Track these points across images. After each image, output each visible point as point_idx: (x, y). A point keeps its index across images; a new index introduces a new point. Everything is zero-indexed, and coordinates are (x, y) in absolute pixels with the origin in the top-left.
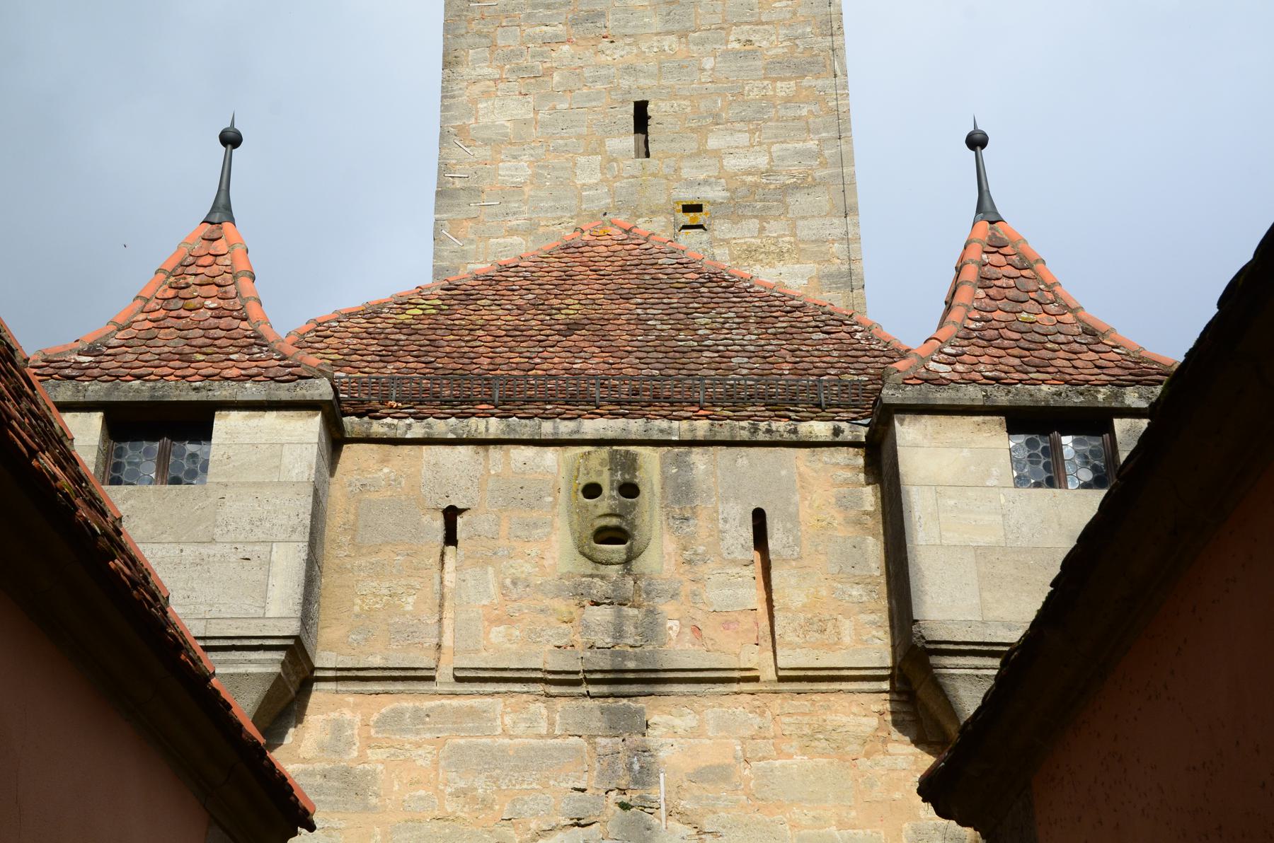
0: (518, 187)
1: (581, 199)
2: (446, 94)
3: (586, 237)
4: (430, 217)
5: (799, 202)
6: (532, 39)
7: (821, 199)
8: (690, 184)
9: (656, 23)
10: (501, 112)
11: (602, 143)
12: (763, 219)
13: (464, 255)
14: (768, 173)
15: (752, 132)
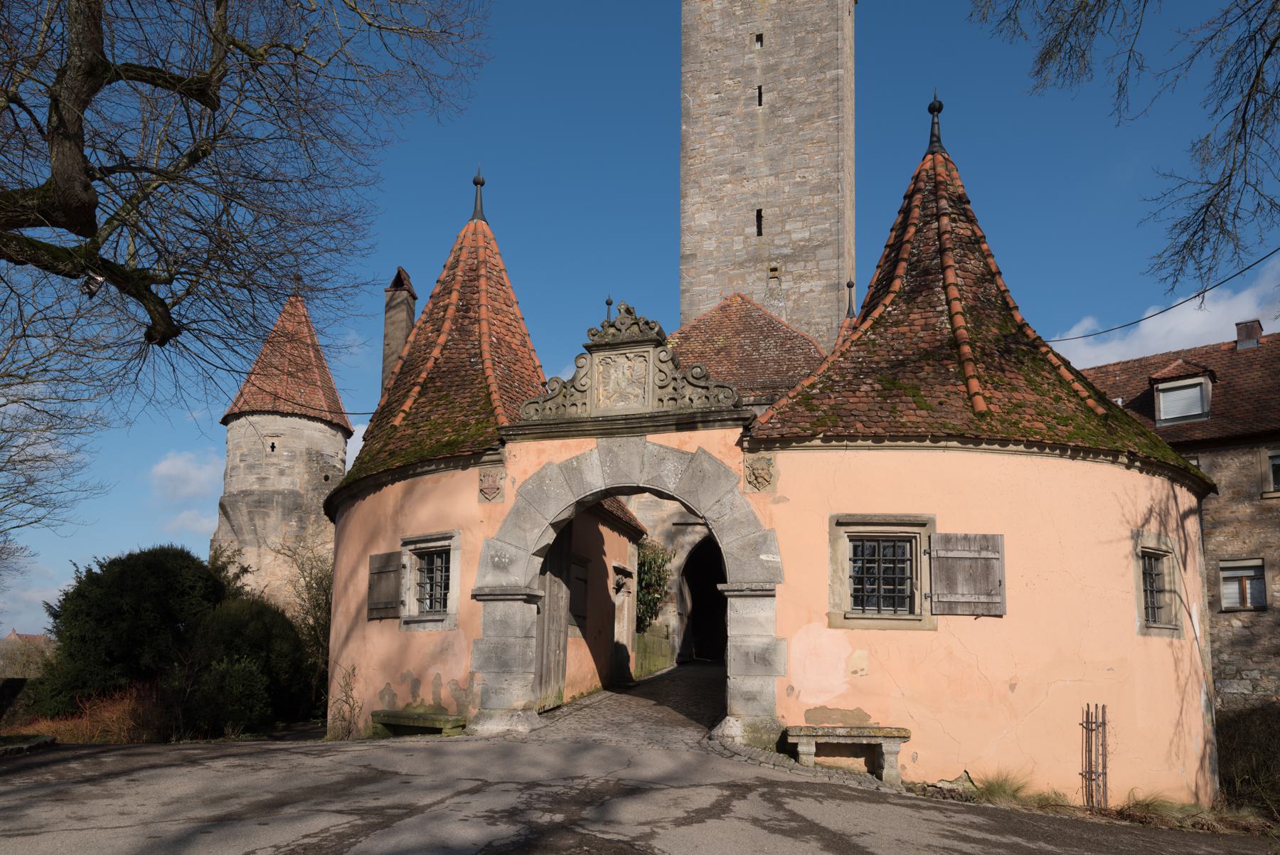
5: (821, 253)
7: (829, 251)
8: (778, 247)
13: (691, 284)
14: (809, 240)
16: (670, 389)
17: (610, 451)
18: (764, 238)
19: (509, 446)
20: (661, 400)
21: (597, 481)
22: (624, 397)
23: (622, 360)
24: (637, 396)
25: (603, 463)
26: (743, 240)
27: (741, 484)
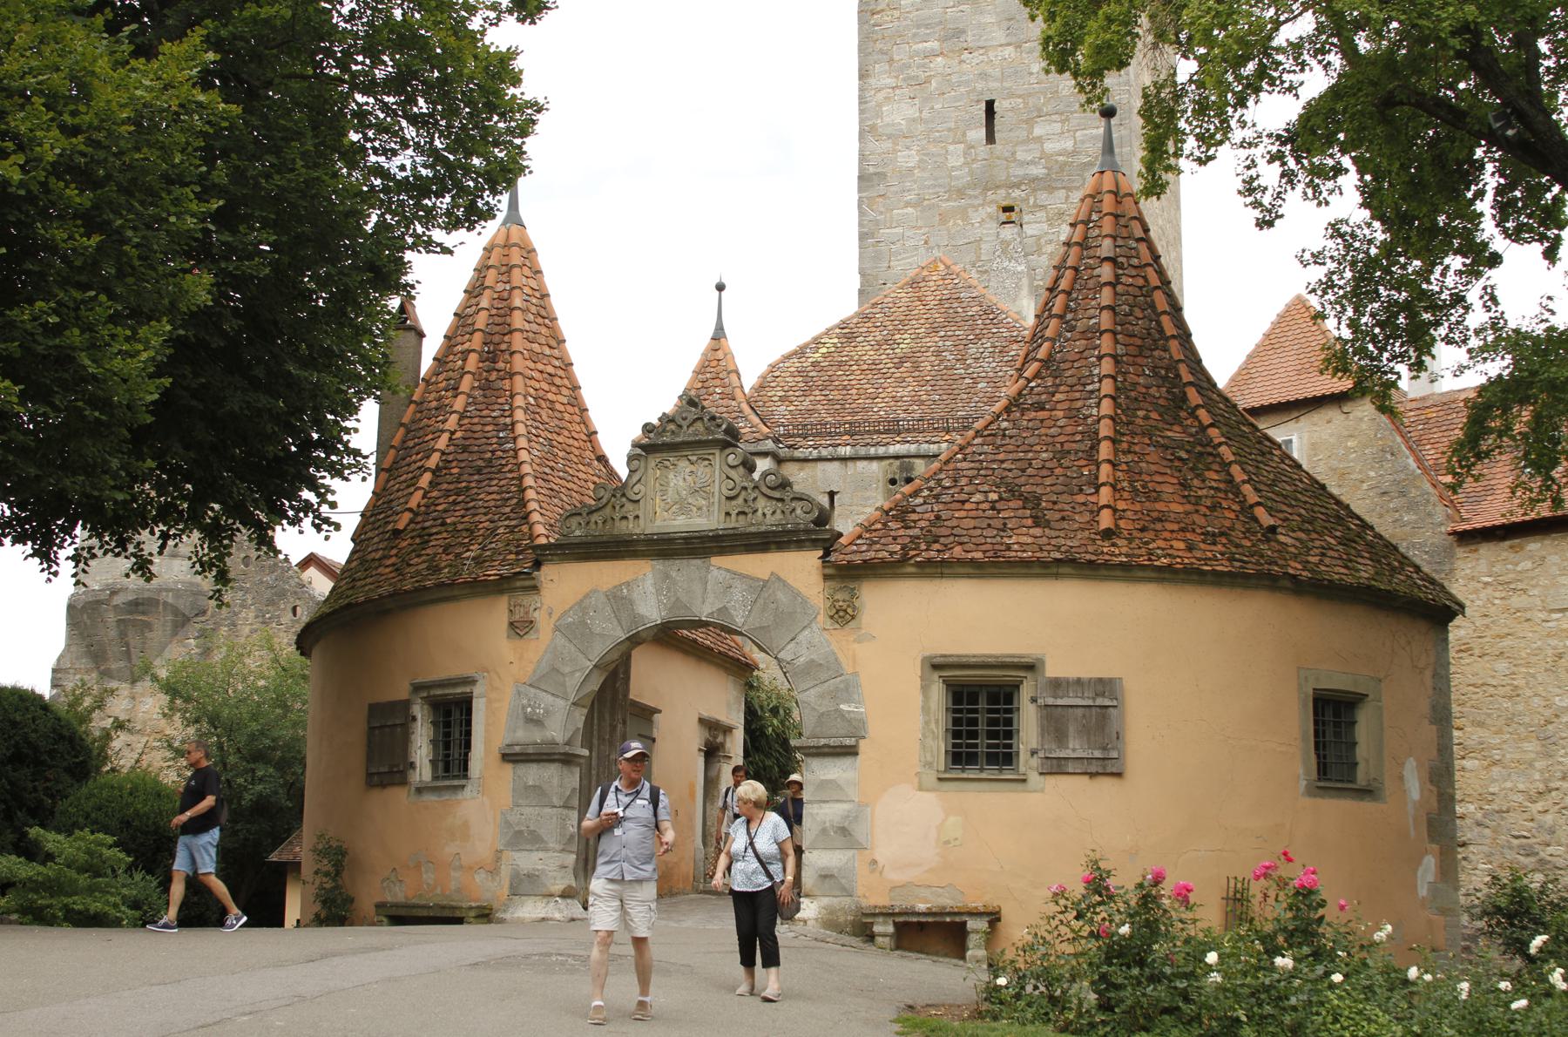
0: (911, 170)
1: (950, 176)
2: (862, 100)
3: (925, 273)
4: (856, 197)
6: (917, 53)
9: (999, 36)
10: (898, 114)
11: (964, 134)
12: (1069, 189)
13: (877, 222)
14: (1075, 153)
15: (1063, 122)
16: (740, 500)
17: (667, 576)
18: (998, 147)
19: (544, 569)
20: (728, 514)
21: (652, 611)
22: (684, 508)
23: (683, 464)
24: (699, 509)
25: (658, 592)
26: (963, 151)
27: (821, 618)
